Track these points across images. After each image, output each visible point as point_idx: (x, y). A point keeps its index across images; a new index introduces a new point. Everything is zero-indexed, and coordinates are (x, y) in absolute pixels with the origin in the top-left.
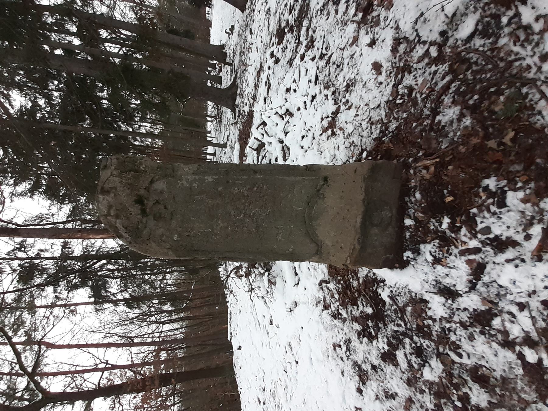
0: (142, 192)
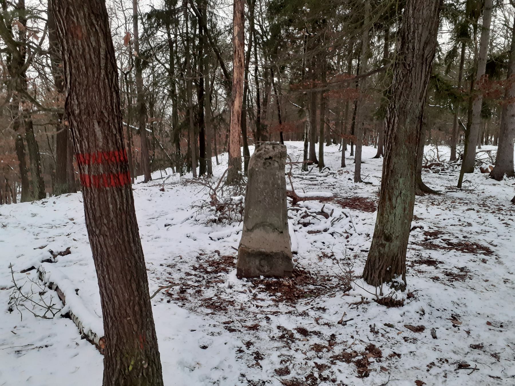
0: (274, 159)
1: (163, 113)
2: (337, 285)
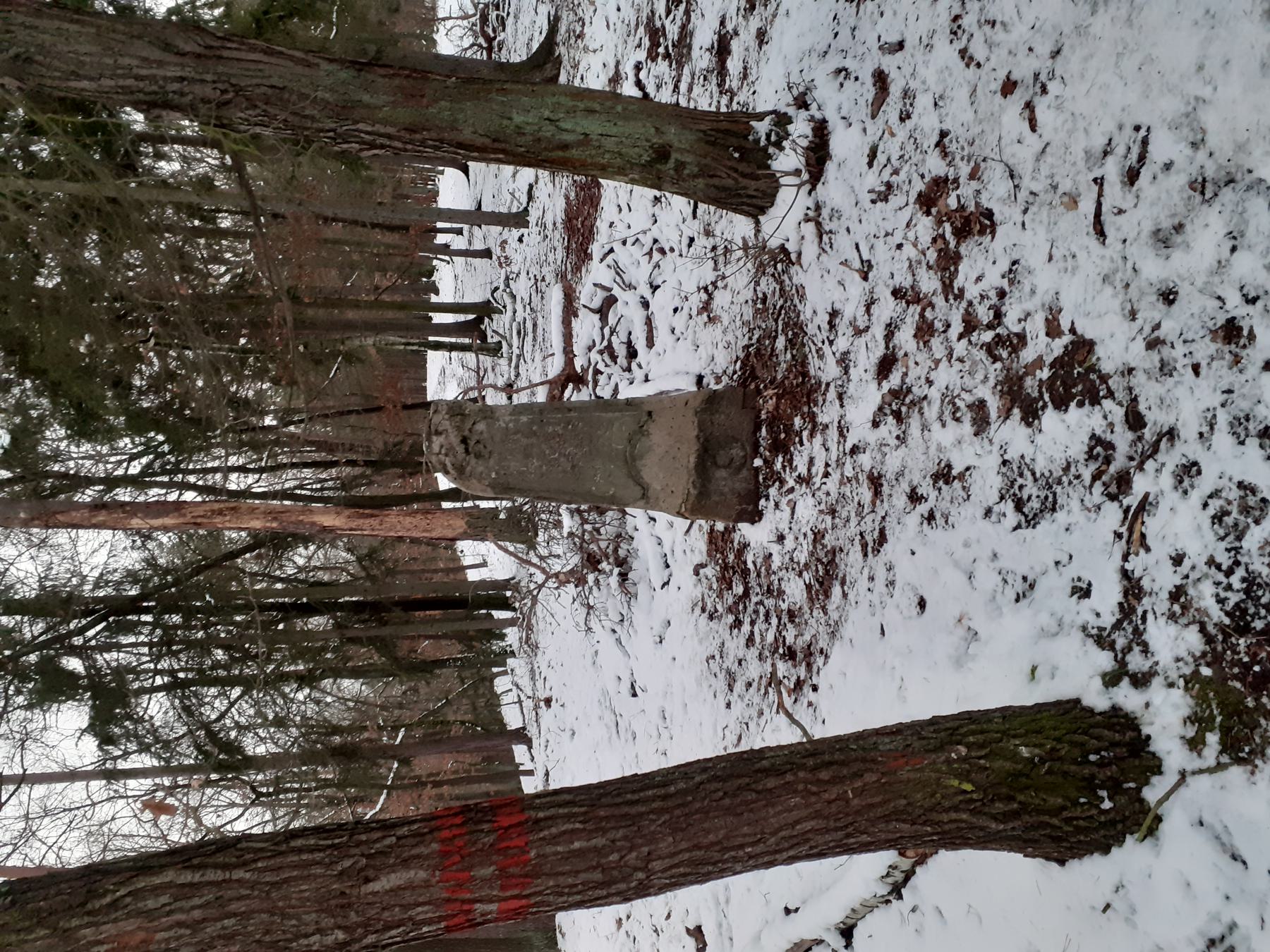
1: (356, 702)
2: (776, 280)
